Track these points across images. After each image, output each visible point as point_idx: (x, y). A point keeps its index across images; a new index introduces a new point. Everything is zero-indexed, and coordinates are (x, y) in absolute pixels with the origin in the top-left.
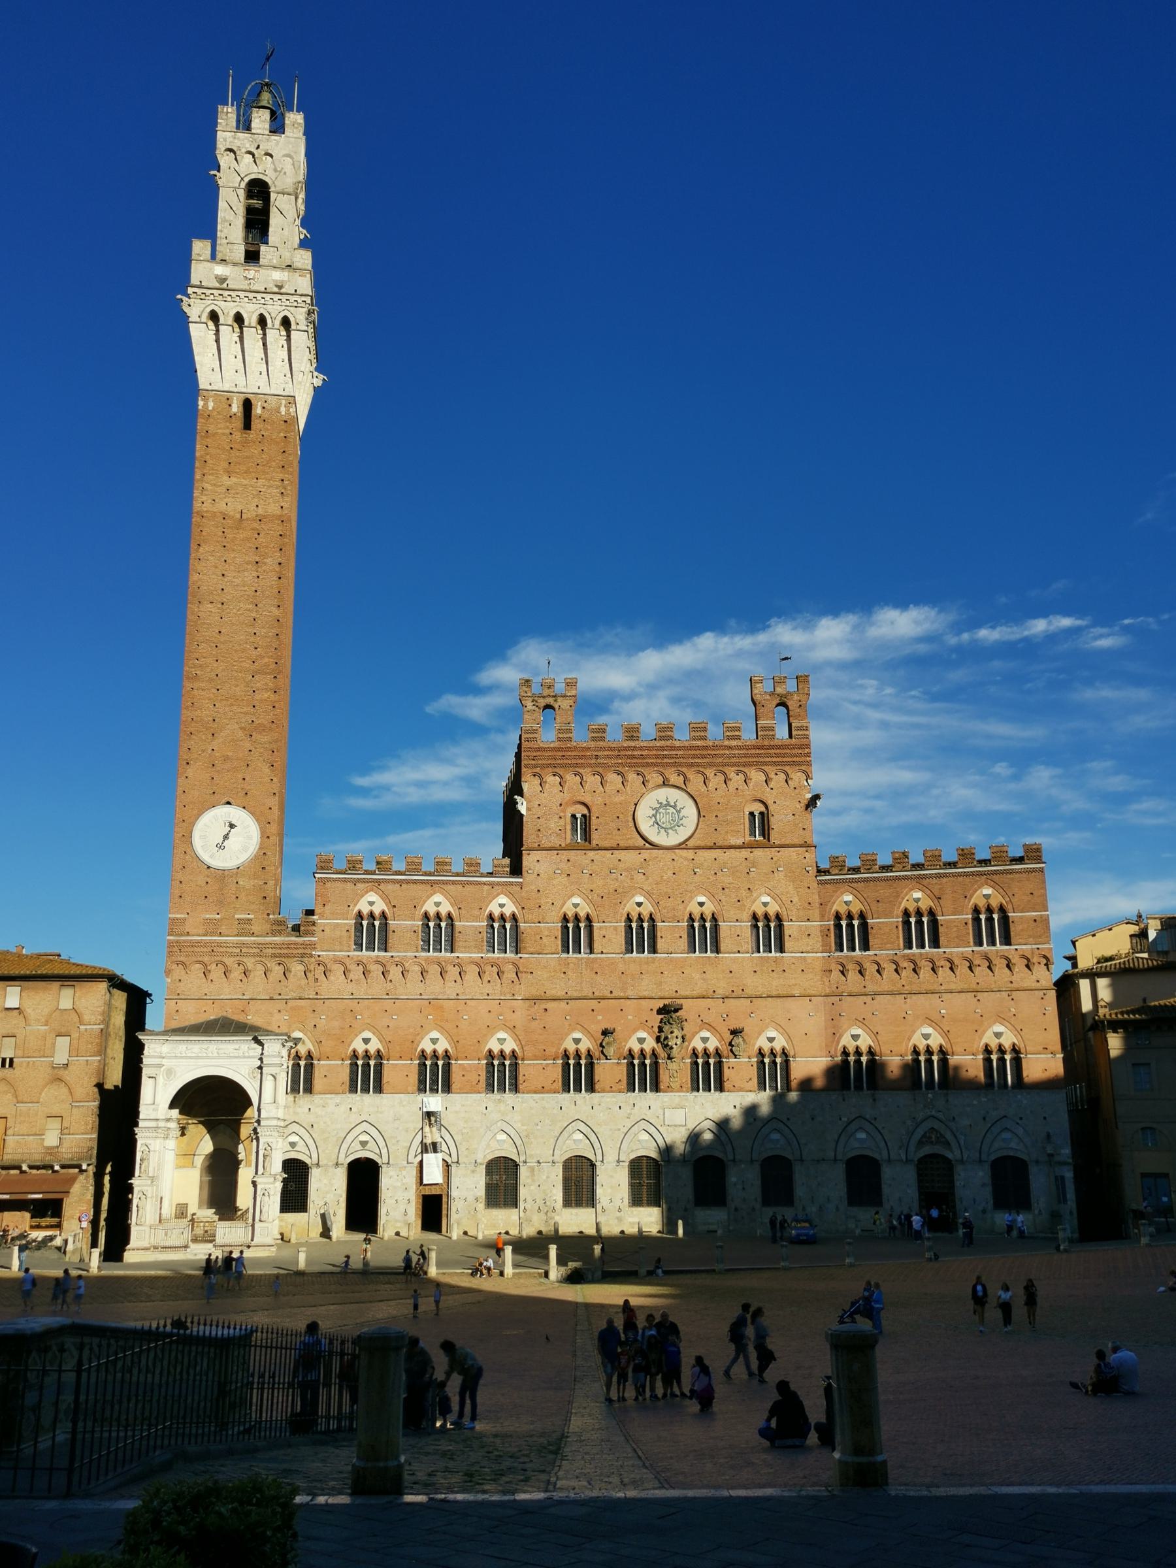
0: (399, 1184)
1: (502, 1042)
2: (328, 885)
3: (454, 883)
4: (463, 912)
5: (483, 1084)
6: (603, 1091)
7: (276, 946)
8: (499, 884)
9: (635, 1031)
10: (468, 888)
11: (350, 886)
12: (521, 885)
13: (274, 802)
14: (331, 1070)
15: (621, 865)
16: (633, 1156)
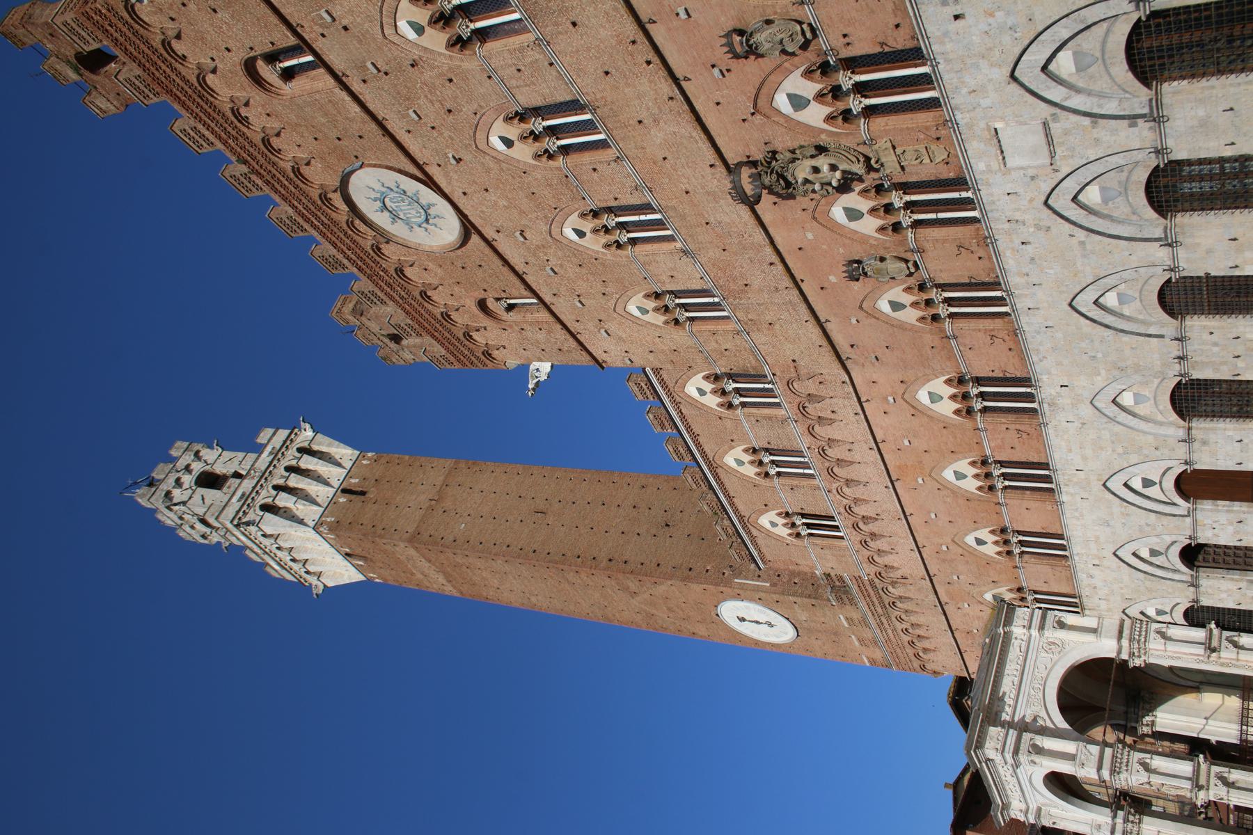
0: (1230, 529)
1: (937, 396)
2: (768, 557)
3: (698, 445)
4: (735, 437)
5: (1025, 423)
6: (993, 269)
7: (870, 604)
8: (669, 394)
9: (833, 227)
10: (696, 430)
11: (760, 541)
12: (657, 371)
13: (696, 588)
14: (1036, 575)
15: (531, 260)
16: (1150, 213)
